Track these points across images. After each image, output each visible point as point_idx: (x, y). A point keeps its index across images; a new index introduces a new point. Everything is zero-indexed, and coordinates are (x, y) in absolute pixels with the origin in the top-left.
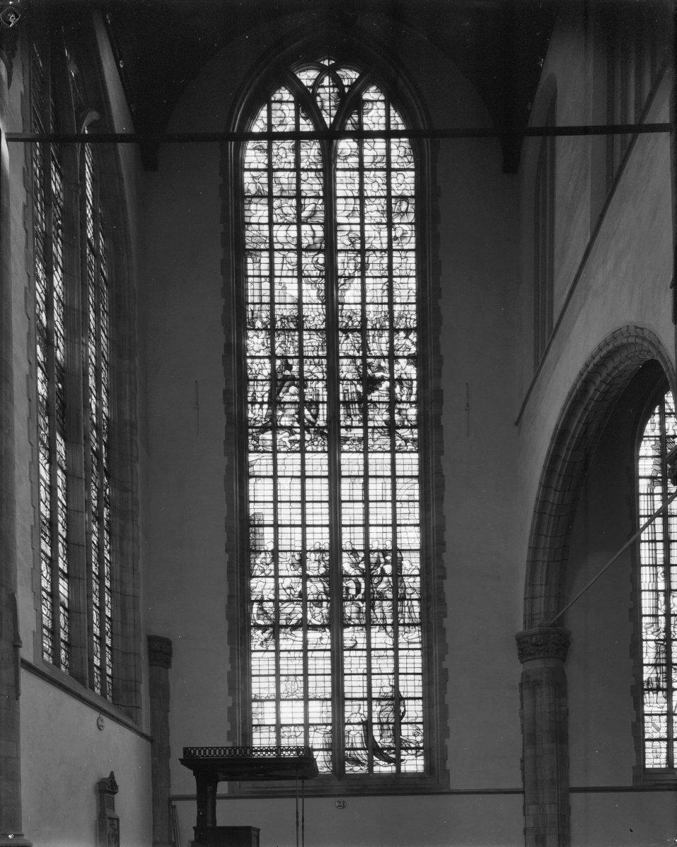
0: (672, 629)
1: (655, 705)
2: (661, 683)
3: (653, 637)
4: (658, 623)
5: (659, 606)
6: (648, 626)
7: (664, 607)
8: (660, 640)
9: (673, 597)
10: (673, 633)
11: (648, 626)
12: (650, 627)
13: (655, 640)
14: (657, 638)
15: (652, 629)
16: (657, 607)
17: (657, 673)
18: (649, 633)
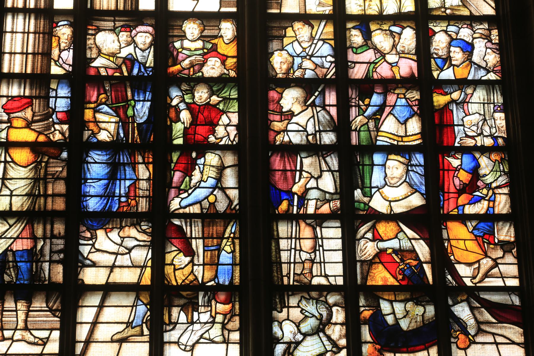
0: (88, 114)
1: (18, 335)
2: (46, 266)
3: (29, 136)
4: (47, 98)
5: (55, 53)
6: (16, 104)
7: (68, 56)
8: (50, 143)
9: (99, 30)
10: (92, 126)
11: (16, 104)
12: (22, 109)
13: (33, 146)
14: (42, 138)
15: (28, 113)
16: (47, 55)
17: (34, 238)
18: (16, 123)
